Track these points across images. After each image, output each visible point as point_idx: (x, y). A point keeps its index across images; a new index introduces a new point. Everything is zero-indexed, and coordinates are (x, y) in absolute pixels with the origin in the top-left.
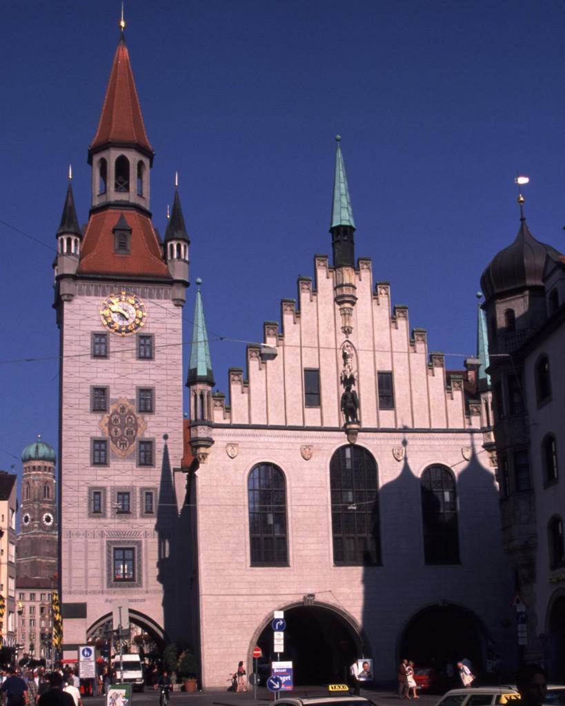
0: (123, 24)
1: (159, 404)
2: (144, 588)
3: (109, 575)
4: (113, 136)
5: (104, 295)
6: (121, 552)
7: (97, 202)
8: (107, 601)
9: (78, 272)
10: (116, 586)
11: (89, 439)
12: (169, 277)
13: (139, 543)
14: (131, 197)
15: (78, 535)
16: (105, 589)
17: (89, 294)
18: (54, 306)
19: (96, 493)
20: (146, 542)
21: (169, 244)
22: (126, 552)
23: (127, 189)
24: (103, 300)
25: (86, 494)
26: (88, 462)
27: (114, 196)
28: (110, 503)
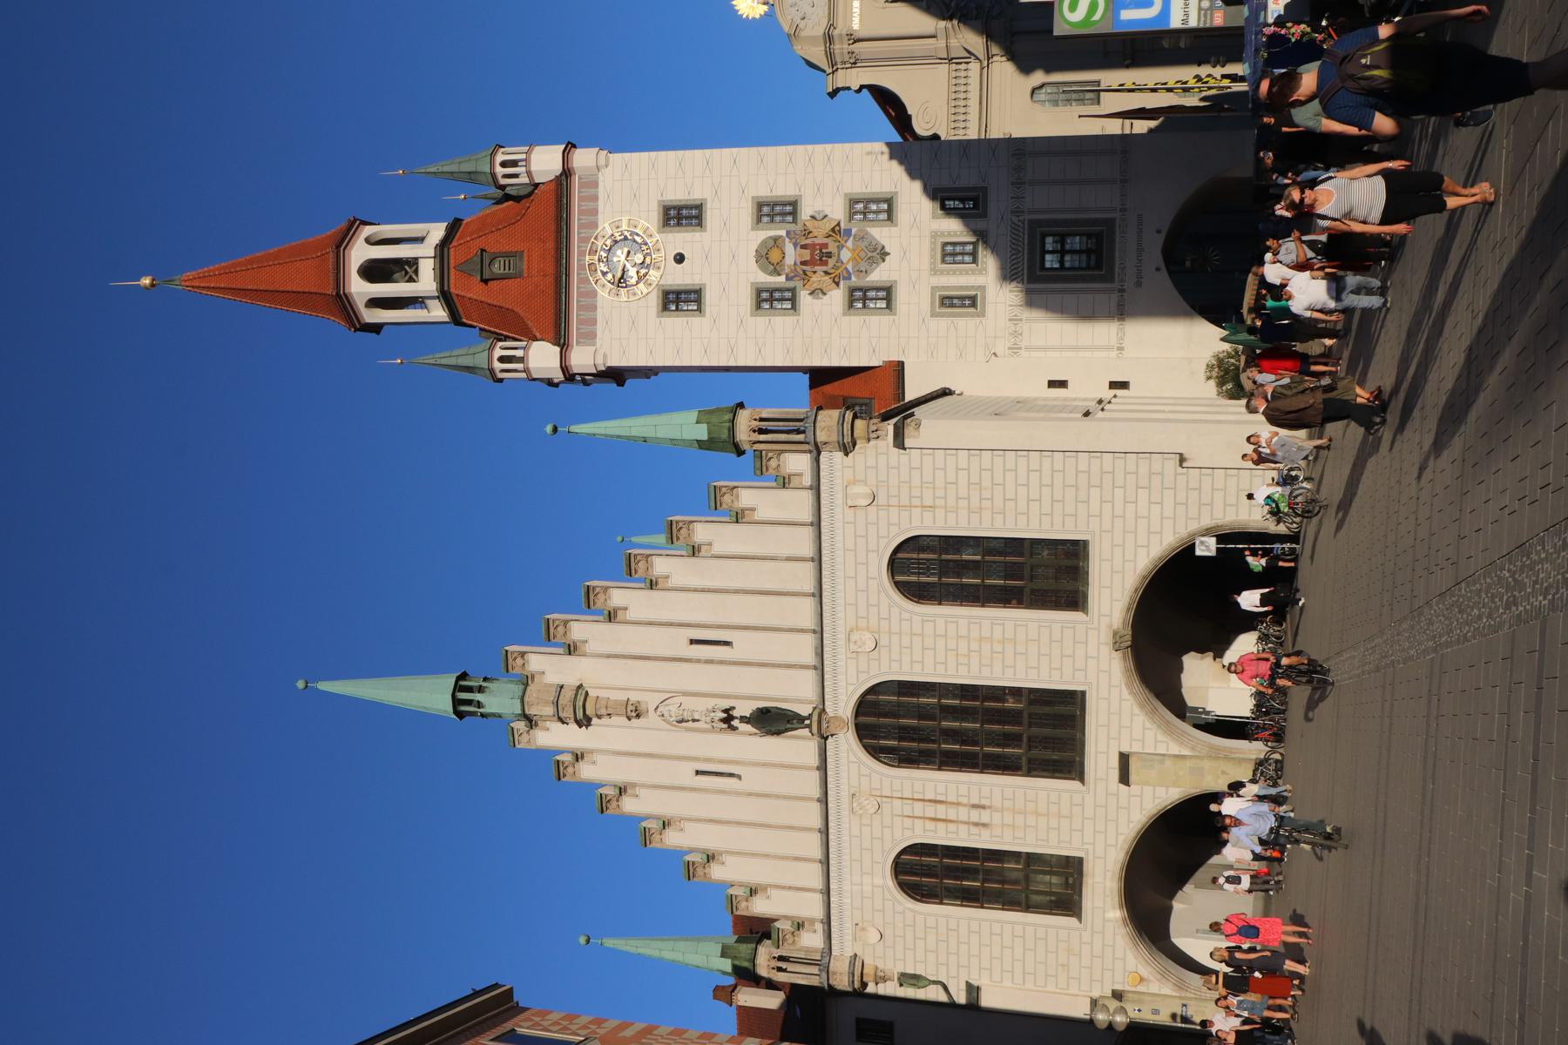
0: (146, 281)
1: (783, 189)
2: (1117, 215)
3: (1093, 279)
5: (594, 294)
6: (1048, 257)
7: (438, 312)
8: (1139, 284)
9: (556, 343)
10: (1112, 268)
11: (847, 318)
12: (558, 178)
13: (1034, 224)
14: (425, 253)
15: (1016, 334)
16: (1116, 285)
17: (594, 322)
18: (621, 383)
19: (942, 304)
20: (1030, 212)
21: (503, 181)
22: (1049, 247)
23: (413, 262)
24: (604, 294)
25: (943, 323)
26: (885, 319)
27: (426, 282)
28: (960, 279)
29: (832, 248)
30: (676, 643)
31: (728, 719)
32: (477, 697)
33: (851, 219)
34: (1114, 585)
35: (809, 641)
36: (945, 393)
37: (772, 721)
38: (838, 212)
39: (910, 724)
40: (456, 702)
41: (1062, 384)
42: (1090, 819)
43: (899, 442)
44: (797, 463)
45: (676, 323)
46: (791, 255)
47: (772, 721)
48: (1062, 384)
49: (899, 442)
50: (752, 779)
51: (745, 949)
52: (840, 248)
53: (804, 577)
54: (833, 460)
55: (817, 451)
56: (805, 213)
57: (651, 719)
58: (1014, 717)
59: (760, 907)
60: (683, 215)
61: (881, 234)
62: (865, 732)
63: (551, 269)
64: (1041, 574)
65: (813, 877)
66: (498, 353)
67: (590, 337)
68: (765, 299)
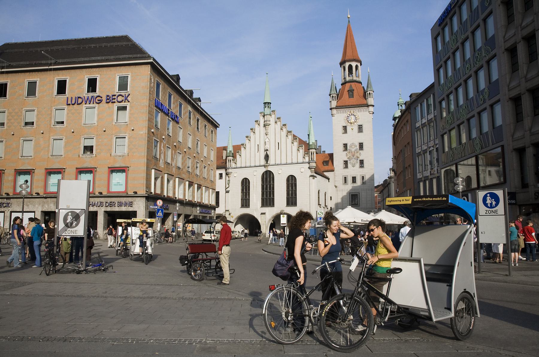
4: (347, 58)
25: (341, 178)
27: (348, 79)
28: (350, 180)
29: (355, 157)
30: (278, 140)
31: (267, 150)
35: (279, 163)
36: (329, 179)
37: (267, 157)
38: (361, 158)
39: (268, 179)
40: (266, 103)
41: (331, 199)
42: (255, 208)
43: (311, 176)
44: (307, 159)
45: (341, 130)
46: (353, 150)
47: (267, 157)
48: (331, 199)
49: (311, 176)
51: (231, 155)
53: (289, 161)
54: (307, 165)
55: (309, 163)
56: (361, 151)
58: (270, 196)
59: (238, 156)
60: (360, 128)
61: (358, 165)
62: (266, 172)
63: (350, 104)
64: (292, 200)
65: (243, 165)
66: (334, 95)
68: (345, 145)
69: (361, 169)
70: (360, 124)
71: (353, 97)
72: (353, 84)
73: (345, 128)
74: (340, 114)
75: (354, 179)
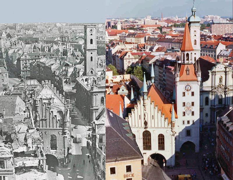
9: (180, 80)
28: (186, 122)
29: (189, 110)
30: (153, 114)
32: (146, 95)
33: (192, 112)
34: (161, 152)
37: (146, 123)
47: (146, 123)
50: (140, 121)
52: (189, 111)
56: (192, 107)
57: (145, 112)
60: (193, 94)
61: (191, 114)
67: (180, 84)
68: (184, 104)
69: (193, 117)
70: (193, 91)
71: (189, 74)
72: (188, 65)
73: (184, 93)
74: (181, 85)
75: (188, 122)
